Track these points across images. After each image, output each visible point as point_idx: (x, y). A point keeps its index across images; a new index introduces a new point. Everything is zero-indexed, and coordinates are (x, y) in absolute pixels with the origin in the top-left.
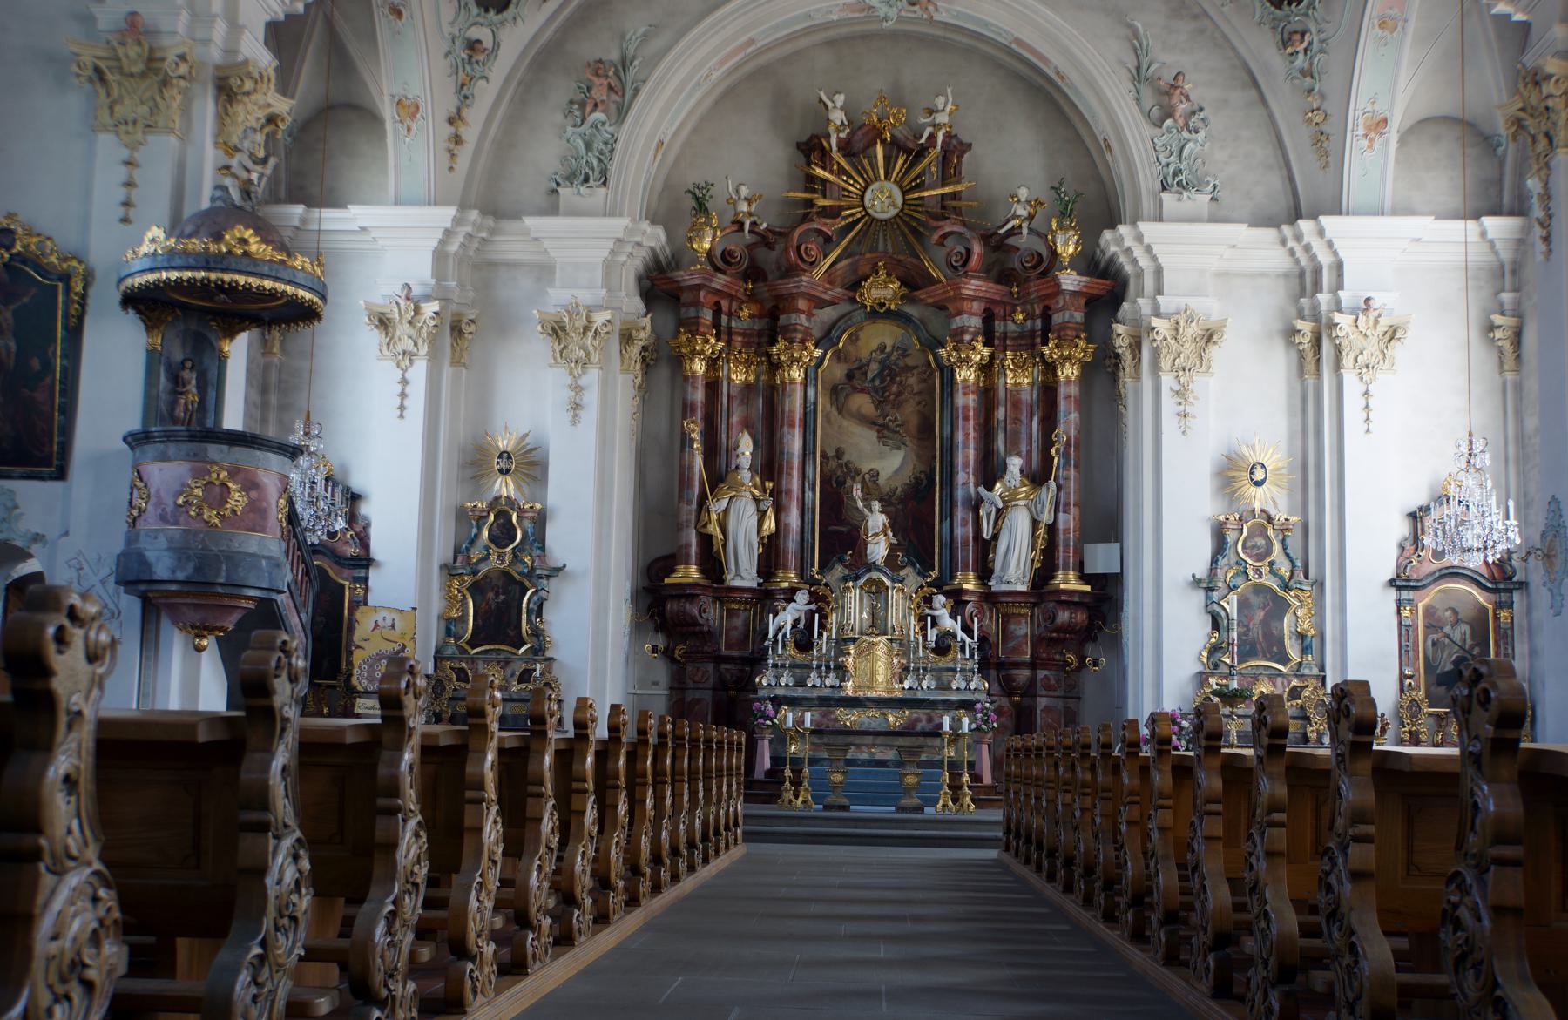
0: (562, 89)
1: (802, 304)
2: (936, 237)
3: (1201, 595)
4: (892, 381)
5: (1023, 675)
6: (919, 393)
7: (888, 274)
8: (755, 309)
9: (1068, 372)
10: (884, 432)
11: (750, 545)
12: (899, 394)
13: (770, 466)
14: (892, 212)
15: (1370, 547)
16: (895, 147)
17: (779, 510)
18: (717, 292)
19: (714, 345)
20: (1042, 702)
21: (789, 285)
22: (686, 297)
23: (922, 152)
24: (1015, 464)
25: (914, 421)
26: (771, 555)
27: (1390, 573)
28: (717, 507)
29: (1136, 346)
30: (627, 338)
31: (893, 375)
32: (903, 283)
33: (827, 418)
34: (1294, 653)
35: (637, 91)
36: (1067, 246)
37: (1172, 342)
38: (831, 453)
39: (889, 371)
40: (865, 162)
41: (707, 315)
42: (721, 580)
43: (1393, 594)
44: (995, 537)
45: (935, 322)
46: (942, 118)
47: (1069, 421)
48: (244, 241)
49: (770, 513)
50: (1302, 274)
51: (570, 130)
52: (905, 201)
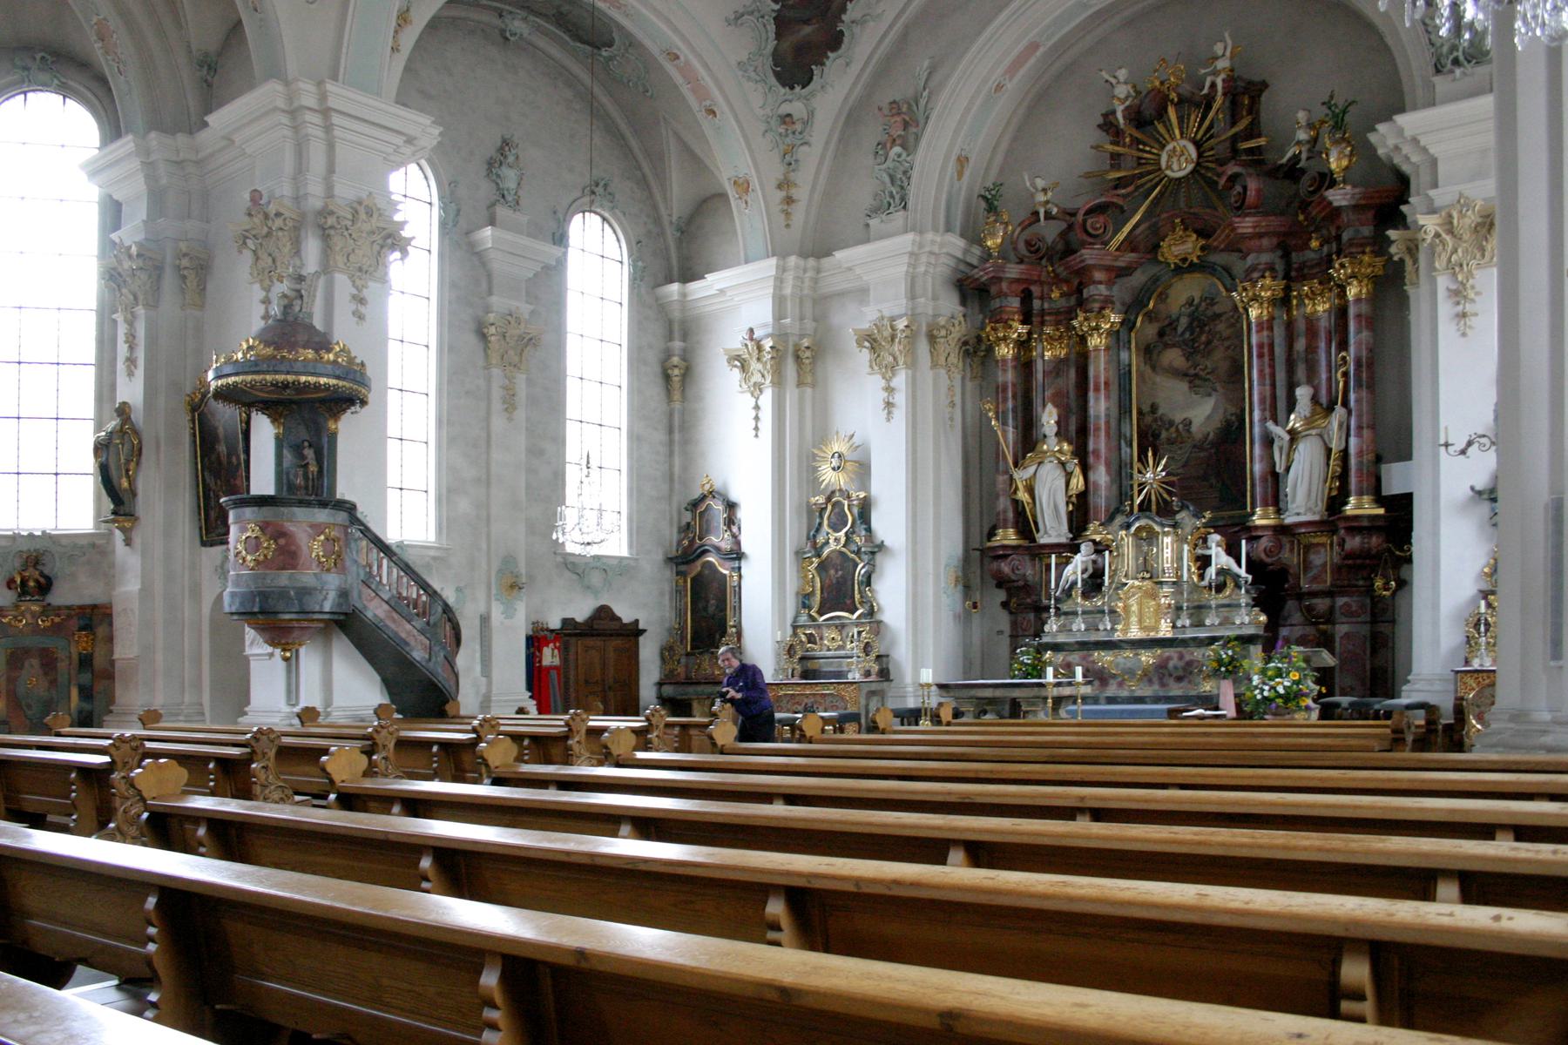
1: (1098, 275)
2: (1222, 181)
4: (1202, 332)
6: (1228, 338)
7: (1186, 229)
10: (1195, 380)
11: (1056, 507)
12: (1208, 343)
13: (1078, 434)
14: (1190, 167)
17: (1085, 469)
18: (1017, 281)
24: (1303, 393)
25: (1224, 366)
31: (1202, 325)
32: (1201, 233)
33: (1141, 375)
36: (1336, 162)
37: (1448, 238)
38: (1146, 409)
40: (1160, 128)
41: (1015, 303)
42: (1033, 540)
44: (1288, 469)
49: (1078, 471)
52: (1200, 155)
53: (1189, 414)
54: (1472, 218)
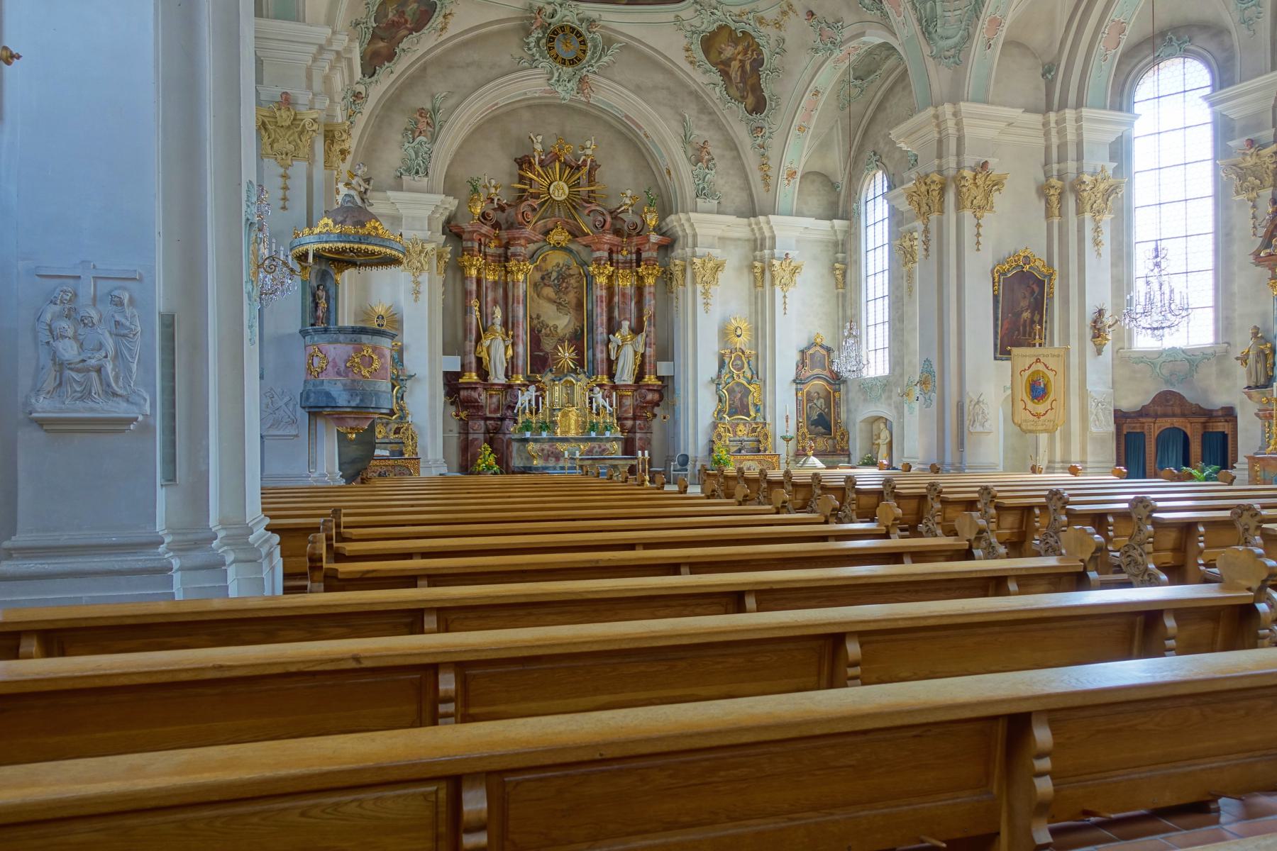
0: (401, 121)
3: (714, 387)
5: (629, 423)
8: (497, 242)
9: (650, 281)
10: (559, 305)
14: (564, 197)
15: (785, 365)
16: (566, 164)
19: (479, 261)
20: (638, 435)
21: (516, 233)
22: (464, 236)
23: (578, 168)
24: (626, 324)
25: (574, 301)
26: (511, 369)
27: (793, 376)
28: (486, 343)
29: (684, 270)
30: (440, 257)
31: (564, 279)
32: (570, 233)
33: (532, 299)
34: (753, 414)
35: (441, 127)
36: (652, 220)
39: (562, 277)
41: (476, 245)
43: (794, 386)
45: (584, 254)
46: (589, 152)
47: (650, 305)
48: (376, 228)
50: (755, 240)
51: (407, 145)
53: (557, 323)
54: (711, 264)
